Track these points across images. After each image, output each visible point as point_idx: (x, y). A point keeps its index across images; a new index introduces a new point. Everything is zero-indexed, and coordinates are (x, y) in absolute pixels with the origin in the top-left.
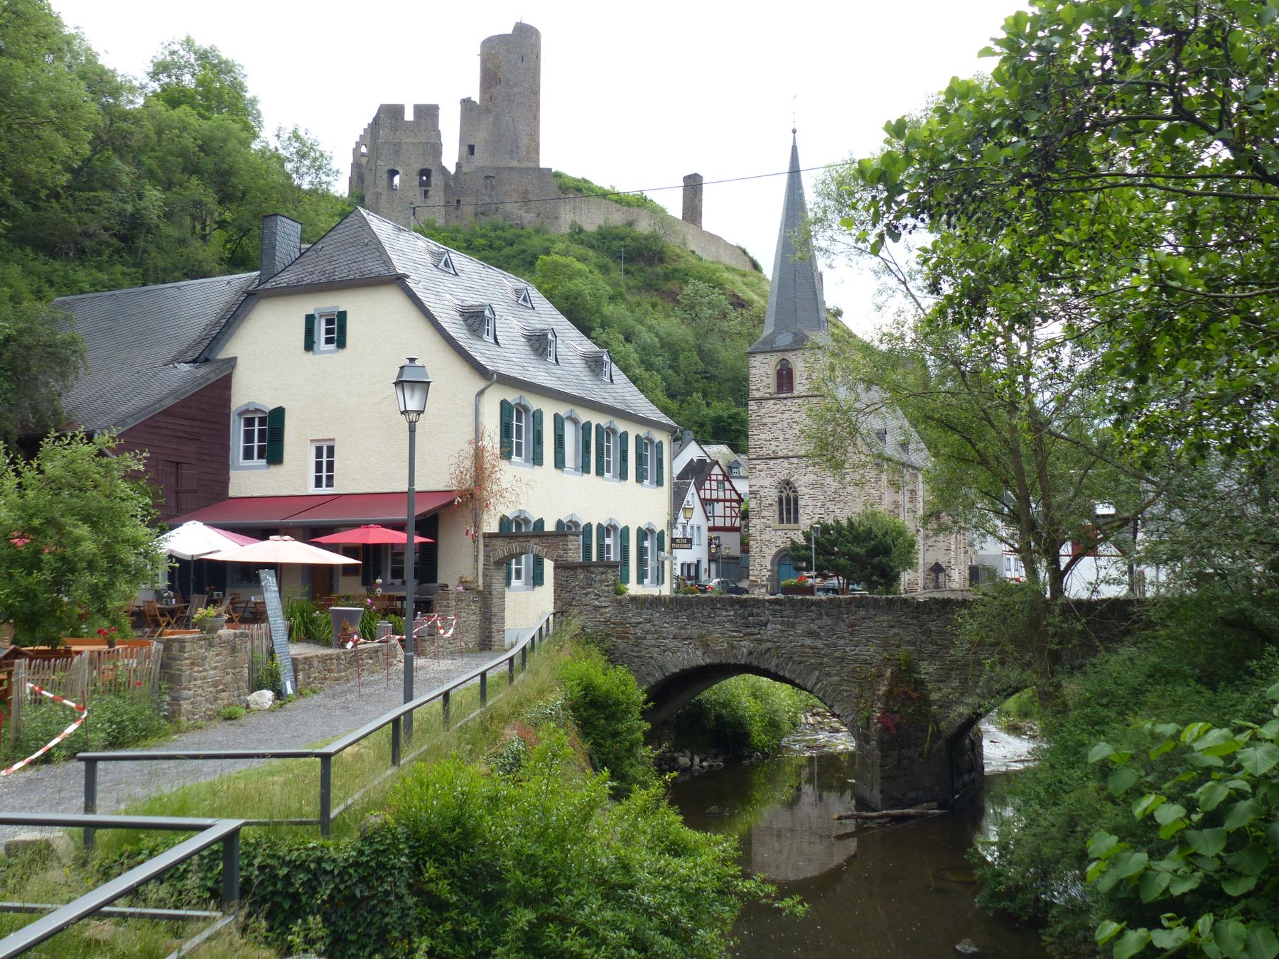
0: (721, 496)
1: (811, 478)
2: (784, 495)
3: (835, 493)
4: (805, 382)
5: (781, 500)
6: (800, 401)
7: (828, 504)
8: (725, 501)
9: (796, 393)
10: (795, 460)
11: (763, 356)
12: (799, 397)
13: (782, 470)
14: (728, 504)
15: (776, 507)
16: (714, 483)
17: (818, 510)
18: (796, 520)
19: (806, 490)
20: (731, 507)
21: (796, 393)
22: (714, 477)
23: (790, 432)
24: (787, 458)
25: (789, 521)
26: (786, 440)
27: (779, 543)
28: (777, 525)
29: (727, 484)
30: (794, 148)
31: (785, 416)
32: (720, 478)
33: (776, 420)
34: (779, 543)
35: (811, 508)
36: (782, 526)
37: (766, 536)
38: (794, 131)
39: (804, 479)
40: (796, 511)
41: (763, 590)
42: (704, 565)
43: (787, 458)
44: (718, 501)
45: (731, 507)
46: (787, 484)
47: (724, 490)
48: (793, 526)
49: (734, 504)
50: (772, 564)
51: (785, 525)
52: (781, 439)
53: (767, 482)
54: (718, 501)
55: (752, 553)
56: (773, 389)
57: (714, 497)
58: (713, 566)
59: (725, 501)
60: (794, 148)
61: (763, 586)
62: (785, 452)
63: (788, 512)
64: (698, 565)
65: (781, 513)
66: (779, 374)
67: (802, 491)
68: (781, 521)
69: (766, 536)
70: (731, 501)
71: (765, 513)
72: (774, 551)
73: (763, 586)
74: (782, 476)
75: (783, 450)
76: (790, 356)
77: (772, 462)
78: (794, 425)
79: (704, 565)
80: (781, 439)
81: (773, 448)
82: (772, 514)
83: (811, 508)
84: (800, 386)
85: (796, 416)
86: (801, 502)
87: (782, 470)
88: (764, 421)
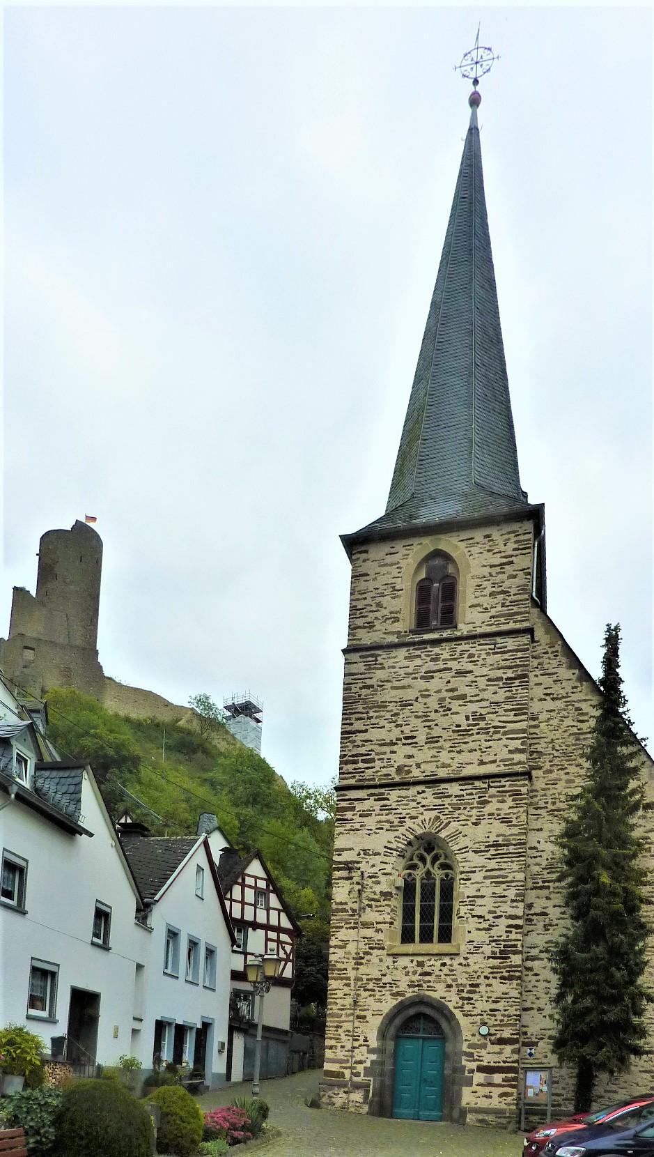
0: (261, 918)
1: (493, 830)
2: (419, 874)
4: (486, 601)
6: (476, 649)
7: (532, 896)
8: (267, 927)
9: (463, 629)
10: (454, 789)
11: (386, 548)
12: (471, 637)
13: (418, 812)
14: (272, 935)
15: (397, 902)
16: (250, 895)
17: (506, 908)
18: (446, 936)
19: (478, 860)
20: (278, 941)
21: (463, 629)
22: (249, 881)
23: (444, 722)
24: (432, 782)
25: (426, 937)
26: (432, 740)
27: (403, 986)
29: (273, 897)
30: (473, 132)
31: (436, 683)
32: (262, 884)
33: (410, 694)
34: (403, 986)
35: (489, 903)
36: (410, 948)
37: (371, 969)
38: (475, 101)
40: (447, 914)
41: (357, 1096)
42: (219, 1034)
44: (255, 925)
45: (278, 941)
46: (428, 847)
47: (268, 909)
48: (436, 947)
49: (284, 937)
50: (382, 1034)
53: (379, 841)
54: (255, 925)
55: (333, 1008)
56: (407, 621)
57: (249, 916)
58: (239, 1042)
59: (267, 927)
60: (473, 132)
61: (357, 1086)
62: (429, 769)
63: (427, 915)
64: (204, 1031)
66: (423, 592)
67: (468, 861)
68: (407, 937)
69: (371, 969)
70: (279, 929)
71: (370, 916)
72: (389, 1004)
73: (357, 1086)
74: (421, 823)
75: (424, 762)
76: (451, 544)
77: (394, 795)
78: (455, 705)
79: (219, 1034)
80: (421, 738)
81: (399, 760)
82: (386, 916)
83: (489, 903)
84: (470, 618)
85: (462, 685)
86: (463, 890)
87: (418, 812)
88: (379, 698)
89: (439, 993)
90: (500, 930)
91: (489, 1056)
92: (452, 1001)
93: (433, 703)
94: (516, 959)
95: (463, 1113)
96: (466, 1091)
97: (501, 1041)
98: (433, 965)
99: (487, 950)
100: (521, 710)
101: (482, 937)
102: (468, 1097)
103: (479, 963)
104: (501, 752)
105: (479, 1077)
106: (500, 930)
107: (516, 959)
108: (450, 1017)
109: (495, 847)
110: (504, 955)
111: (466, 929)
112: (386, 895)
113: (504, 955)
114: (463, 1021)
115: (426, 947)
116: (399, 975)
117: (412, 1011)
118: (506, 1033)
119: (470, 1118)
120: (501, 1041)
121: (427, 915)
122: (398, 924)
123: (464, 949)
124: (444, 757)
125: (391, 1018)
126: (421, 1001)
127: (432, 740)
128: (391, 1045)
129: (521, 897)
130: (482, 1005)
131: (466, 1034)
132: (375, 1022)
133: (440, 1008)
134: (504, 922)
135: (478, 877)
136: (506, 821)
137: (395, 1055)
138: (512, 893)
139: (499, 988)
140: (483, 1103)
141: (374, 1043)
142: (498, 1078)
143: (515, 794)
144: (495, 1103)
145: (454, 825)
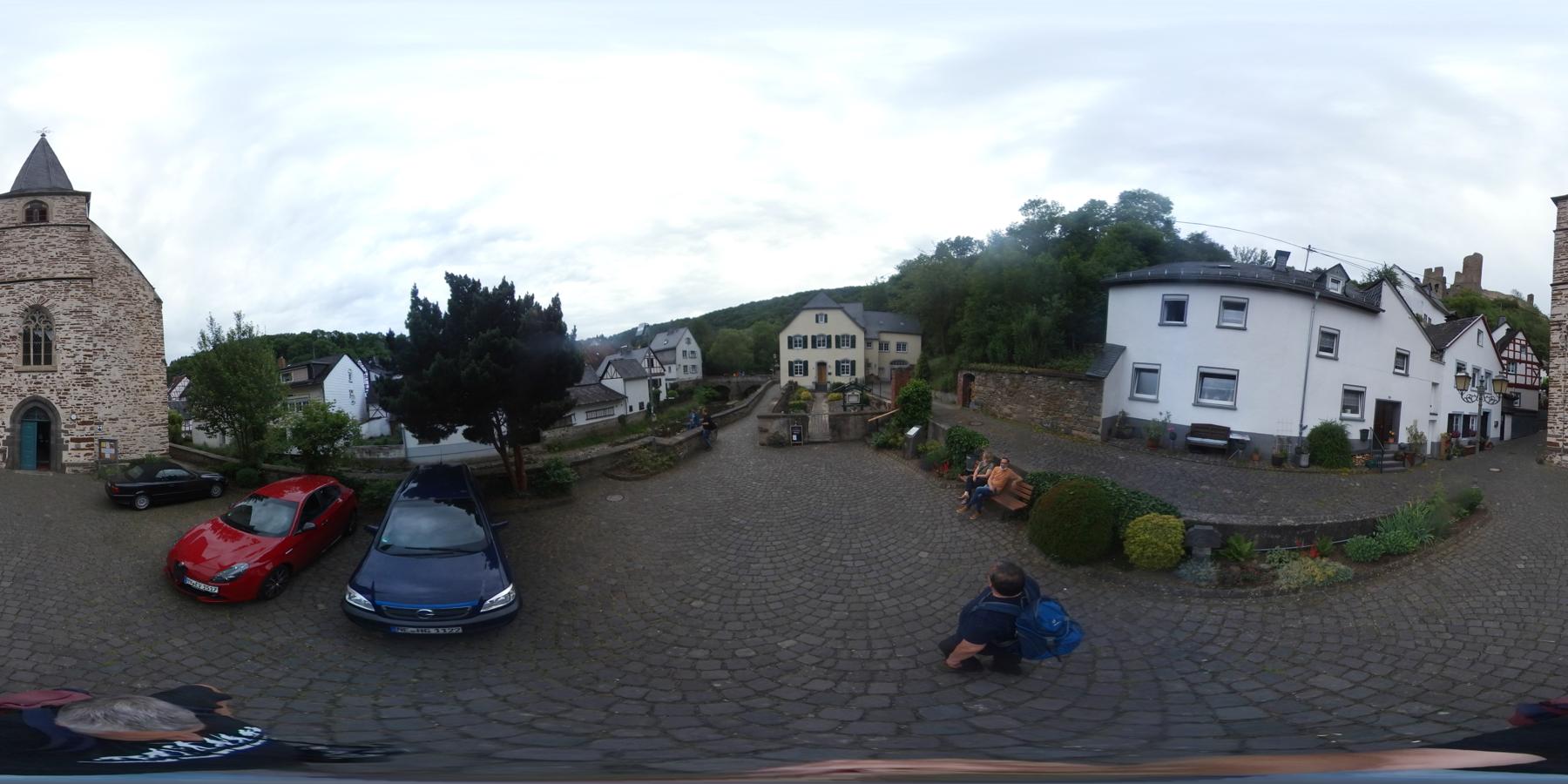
1: (75, 304)
2: (32, 326)
3: (105, 326)
5: (26, 336)
7: (96, 340)
10: (51, 283)
15: (20, 342)
17: (83, 345)
19: (67, 319)
24: (38, 280)
25: (37, 361)
27: (25, 390)
28: (20, 366)
34: (25, 390)
35: (73, 342)
39: (62, 307)
43: (38, 280)
48: (43, 367)
50: (13, 420)
51: (32, 367)
52: (31, 260)
62: (36, 275)
63: (37, 349)
65: (26, 349)
68: (26, 361)
72: (16, 401)
74: (34, 299)
75: (33, 271)
77: (16, 286)
80: (31, 260)
83: (73, 342)
89: (46, 394)
90: (80, 358)
91: (77, 432)
92: (54, 399)
93: (37, 247)
94: (90, 374)
95: (64, 466)
96: (65, 454)
97: (84, 423)
98: (42, 377)
99: (74, 369)
100: (86, 253)
101: (71, 361)
102: (66, 457)
103: (69, 376)
104: (76, 269)
105: (72, 445)
106: (80, 358)
107: (90, 374)
108: (53, 409)
109: (75, 312)
110: (83, 372)
111: (61, 357)
112: (13, 338)
113: (83, 372)
114: (61, 412)
115: (37, 367)
116: (22, 384)
117: (31, 405)
118: (86, 418)
119: (68, 470)
120: (84, 423)
121: (37, 349)
122: (21, 354)
123: (60, 368)
124: (45, 269)
125: (17, 410)
126: (36, 399)
127: (36, 262)
128: (18, 426)
129: (90, 340)
130: (72, 402)
131: (63, 419)
132: (9, 413)
133: (47, 403)
134: (82, 353)
135: (66, 327)
136: (80, 299)
137: (21, 431)
138: (86, 337)
139: (81, 391)
140: (75, 460)
141: (8, 426)
142: (83, 445)
143: (85, 288)
144: (82, 459)
145: (52, 301)
